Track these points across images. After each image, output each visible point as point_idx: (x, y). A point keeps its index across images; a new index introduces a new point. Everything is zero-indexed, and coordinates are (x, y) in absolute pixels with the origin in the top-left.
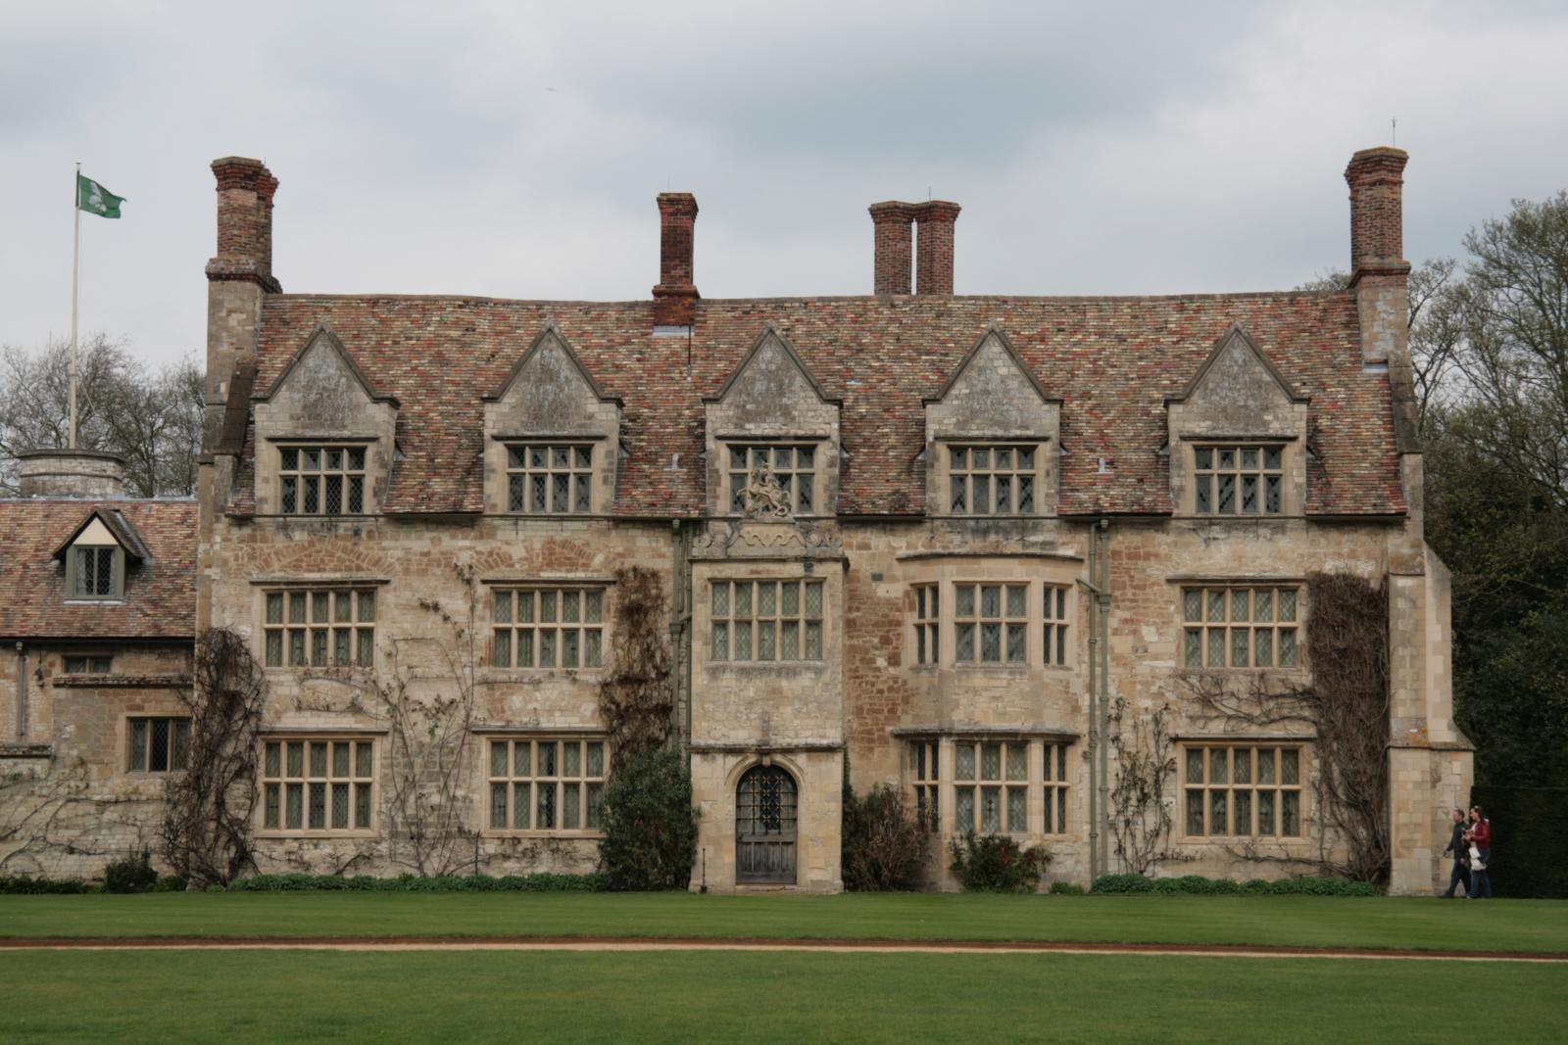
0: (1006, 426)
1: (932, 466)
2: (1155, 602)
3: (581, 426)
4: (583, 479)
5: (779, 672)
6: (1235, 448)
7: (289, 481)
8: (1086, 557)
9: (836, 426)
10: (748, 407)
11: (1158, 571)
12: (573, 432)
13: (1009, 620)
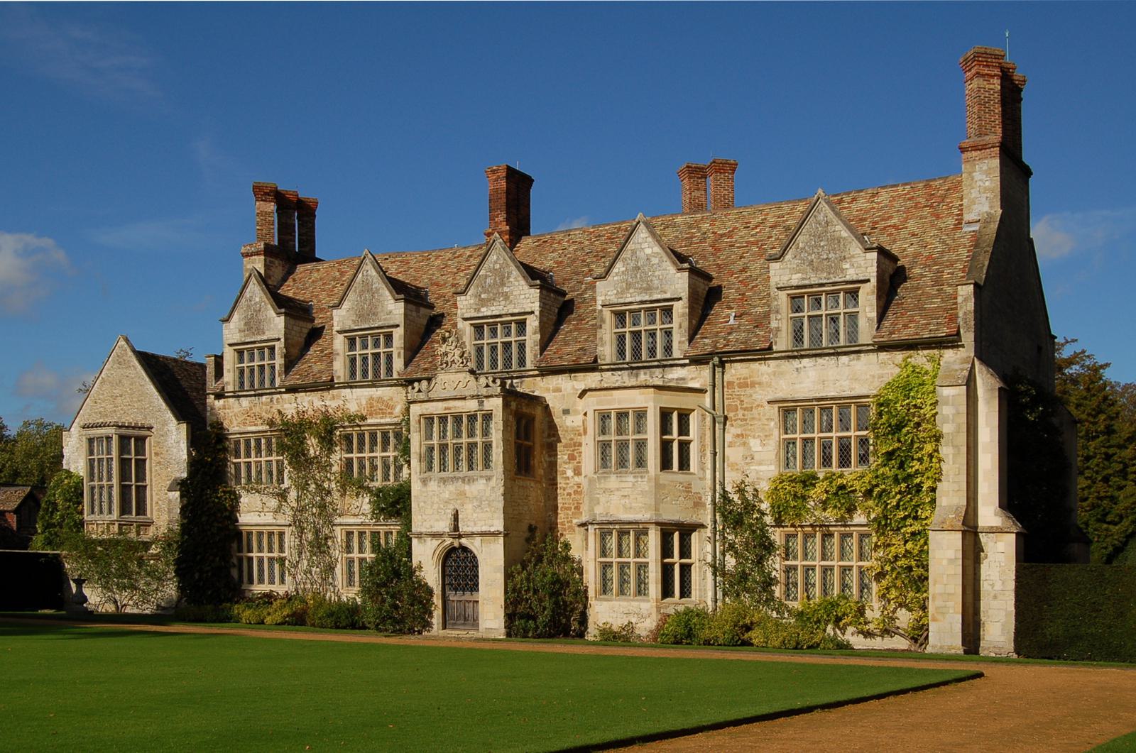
0: (649, 289)
1: (601, 327)
2: (760, 420)
3: (385, 319)
4: (389, 357)
5: (463, 480)
6: (820, 293)
7: (242, 372)
8: (709, 389)
9: (537, 304)
10: (483, 296)
11: (761, 395)
12: (380, 324)
13: (634, 437)
